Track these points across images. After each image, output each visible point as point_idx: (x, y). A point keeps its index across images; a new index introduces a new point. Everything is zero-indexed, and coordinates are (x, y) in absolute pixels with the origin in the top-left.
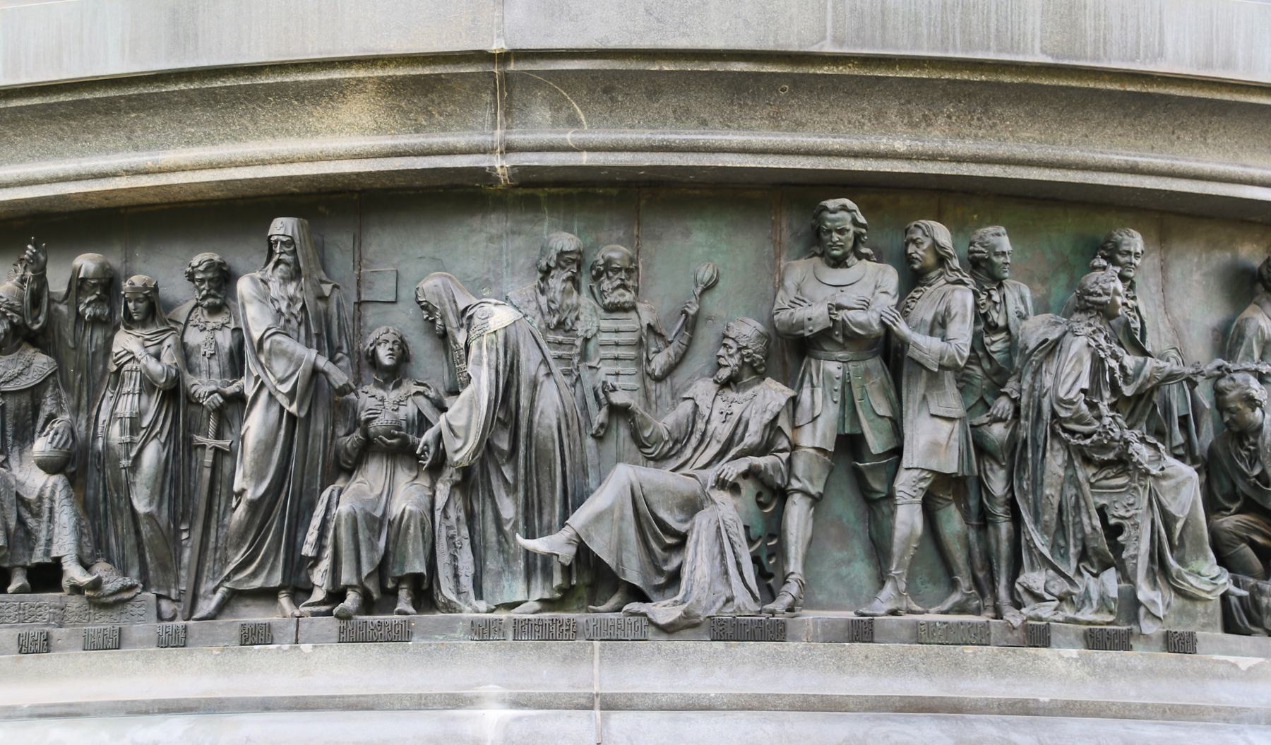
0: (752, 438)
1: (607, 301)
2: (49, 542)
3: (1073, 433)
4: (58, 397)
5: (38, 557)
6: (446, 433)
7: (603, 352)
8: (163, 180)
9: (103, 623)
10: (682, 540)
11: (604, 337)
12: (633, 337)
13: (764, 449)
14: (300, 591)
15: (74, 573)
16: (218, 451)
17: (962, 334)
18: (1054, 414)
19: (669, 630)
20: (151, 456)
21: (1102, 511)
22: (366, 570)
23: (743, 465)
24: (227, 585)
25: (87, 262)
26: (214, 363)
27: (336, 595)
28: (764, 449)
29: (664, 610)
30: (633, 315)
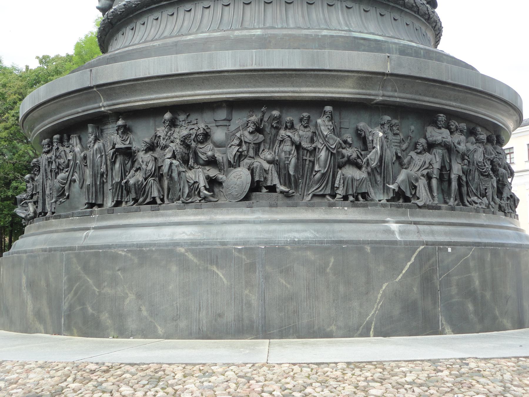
0: (427, 165)
1: (395, 132)
2: (272, 180)
3: (480, 168)
4: (264, 145)
6: (369, 159)
7: (393, 144)
8: (301, 95)
9: (289, 201)
11: (393, 141)
12: (398, 141)
14: (333, 196)
18: (477, 164)
19: (420, 207)
20: (293, 161)
24: (313, 193)
25: (276, 113)
26: (308, 139)
30: (399, 136)
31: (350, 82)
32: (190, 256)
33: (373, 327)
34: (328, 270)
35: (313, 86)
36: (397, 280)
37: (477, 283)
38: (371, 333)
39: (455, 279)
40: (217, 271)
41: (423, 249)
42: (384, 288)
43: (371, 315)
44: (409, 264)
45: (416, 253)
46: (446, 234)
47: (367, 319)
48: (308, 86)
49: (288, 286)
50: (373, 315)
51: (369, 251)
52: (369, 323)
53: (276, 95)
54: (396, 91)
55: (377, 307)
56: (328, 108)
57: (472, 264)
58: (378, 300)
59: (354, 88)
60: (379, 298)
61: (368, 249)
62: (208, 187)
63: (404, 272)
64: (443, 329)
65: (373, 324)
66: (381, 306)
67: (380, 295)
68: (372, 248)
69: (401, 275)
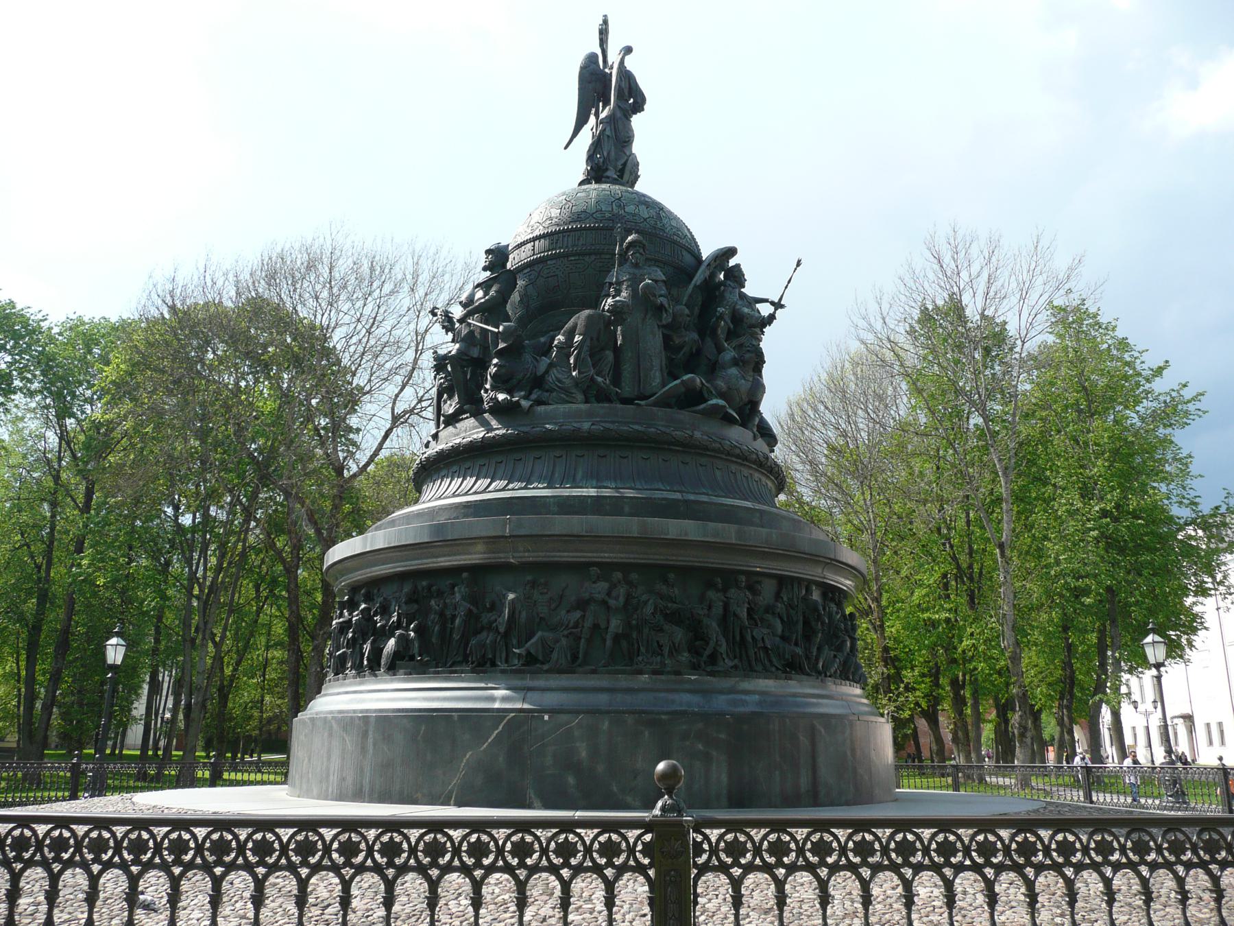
0: (571, 624)
17: (622, 600)
19: (547, 672)
21: (658, 642)
29: (546, 667)
34: (419, 738)
37: (584, 754)
52: (451, 792)
56: (465, 575)
57: (576, 733)
64: (532, 803)
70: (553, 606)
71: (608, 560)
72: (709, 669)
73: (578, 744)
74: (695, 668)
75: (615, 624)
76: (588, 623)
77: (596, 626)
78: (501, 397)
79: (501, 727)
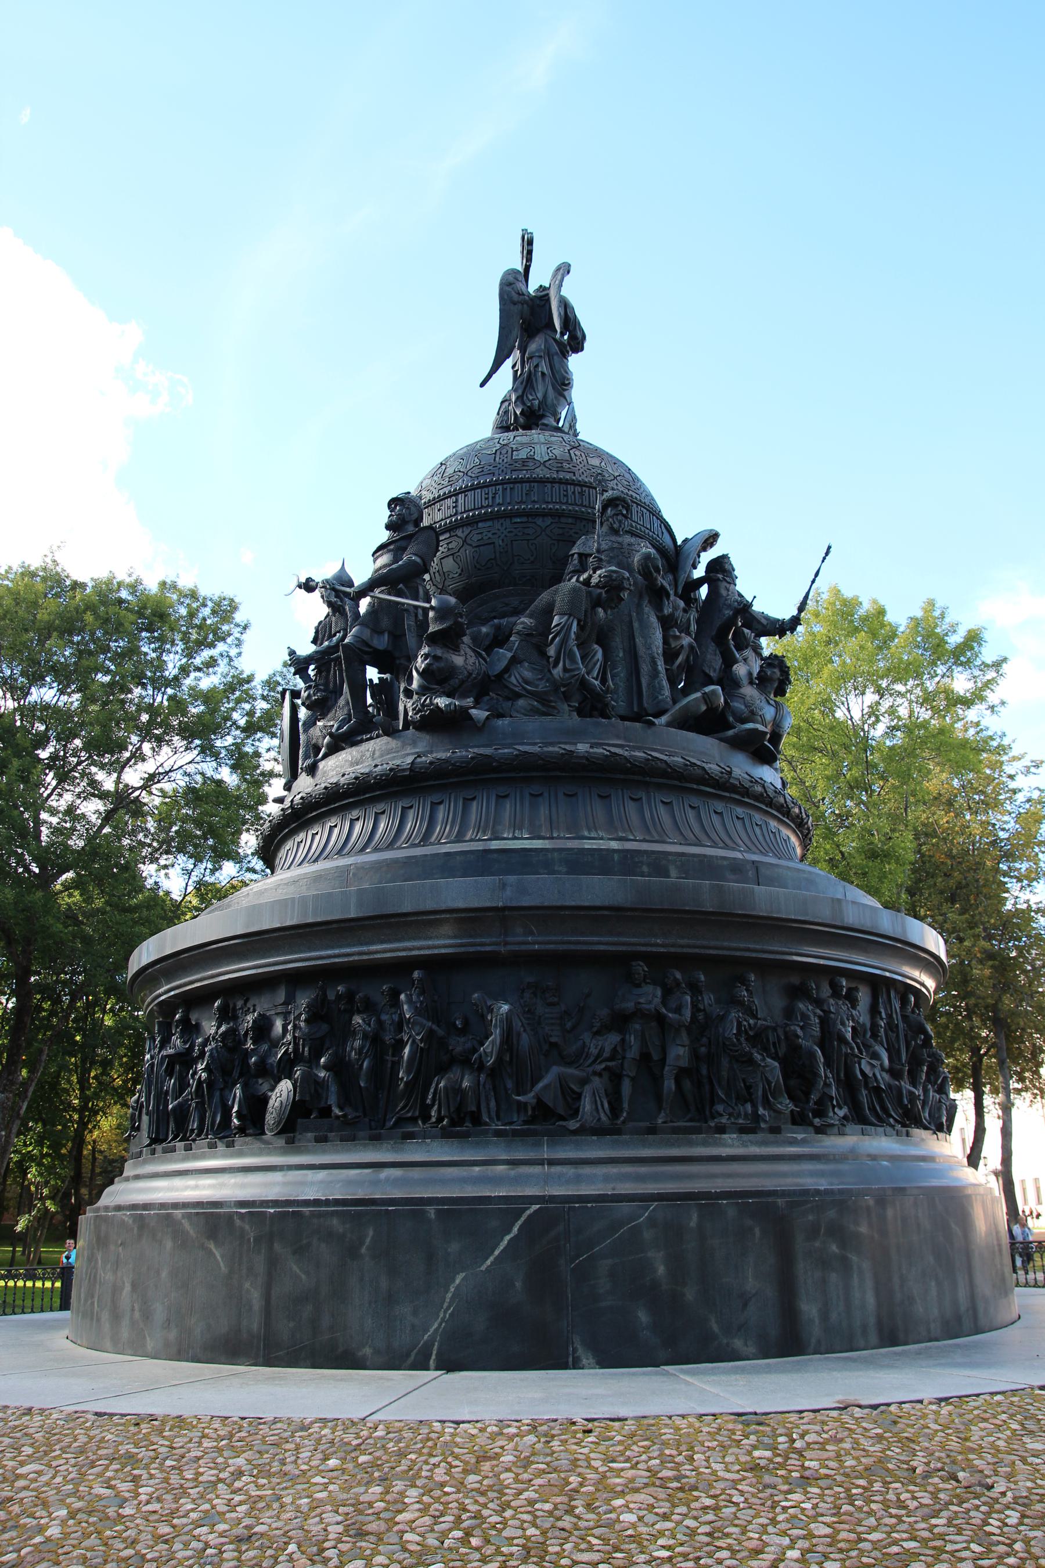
0: (606, 1054)
2: (327, 1099)
5: (322, 1104)
10: (578, 1097)
13: (612, 1058)
15: (337, 1111)
16: (393, 1062)
17: (687, 1013)
18: (724, 1044)
19: (575, 1133)
21: (744, 1081)
22: (452, 1110)
23: (603, 1066)
27: (440, 1119)
28: (612, 1058)
29: (573, 1125)
31: (446, 929)
32: (186, 1225)
33: (434, 1352)
34: (363, 1250)
35: (389, 941)
36: (483, 1268)
37: (661, 1270)
38: (432, 1363)
39: (605, 1265)
40: (214, 1250)
41: (536, 1211)
42: (457, 1281)
43: (432, 1330)
44: (508, 1238)
45: (522, 1219)
46: (607, 1179)
47: (426, 1337)
48: (382, 942)
49: (303, 1276)
50: (437, 1330)
51: (433, 1216)
52: (428, 1346)
53: (337, 960)
54: (532, 933)
55: (445, 1316)
57: (647, 1235)
58: (445, 1305)
59: (455, 937)
60: (448, 1300)
61: (431, 1211)
62: (245, 1112)
63: (497, 1253)
65: (436, 1347)
66: (451, 1315)
67: (449, 1295)
68: (438, 1211)
69: (492, 1258)
70: (569, 1025)
71: (662, 950)
72: (817, 1121)
73: (650, 1254)
74: (799, 1120)
75: (679, 1053)
76: (633, 1053)
77: (645, 1057)
78: (441, 702)
79: (515, 1230)
